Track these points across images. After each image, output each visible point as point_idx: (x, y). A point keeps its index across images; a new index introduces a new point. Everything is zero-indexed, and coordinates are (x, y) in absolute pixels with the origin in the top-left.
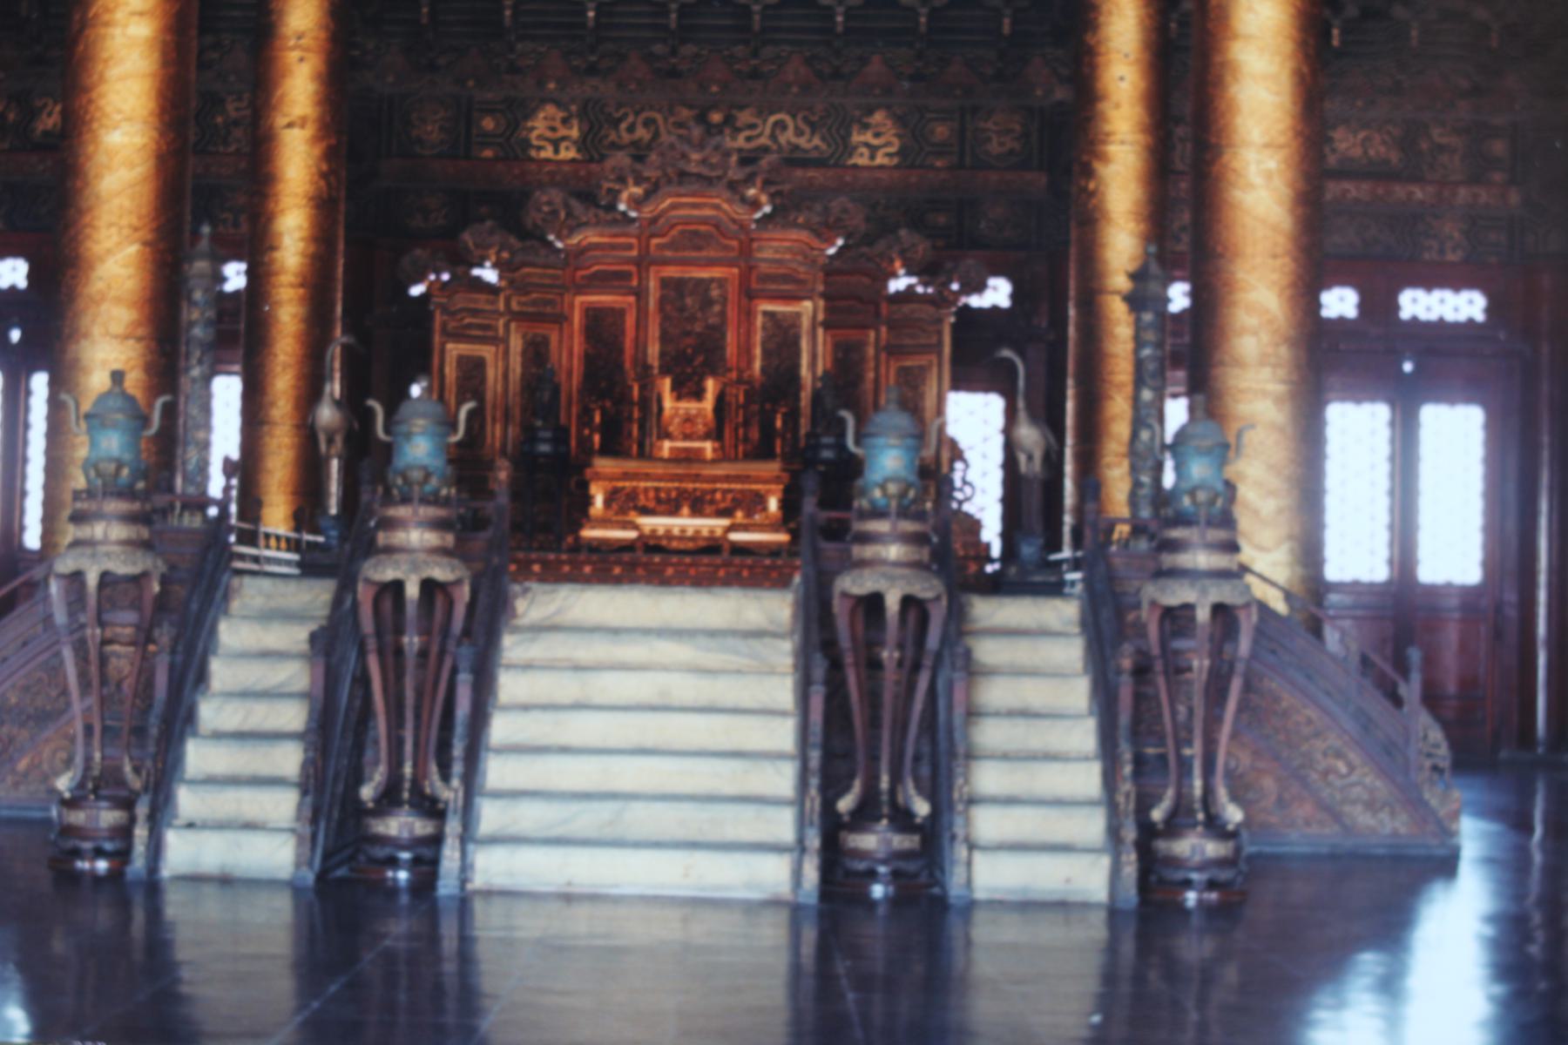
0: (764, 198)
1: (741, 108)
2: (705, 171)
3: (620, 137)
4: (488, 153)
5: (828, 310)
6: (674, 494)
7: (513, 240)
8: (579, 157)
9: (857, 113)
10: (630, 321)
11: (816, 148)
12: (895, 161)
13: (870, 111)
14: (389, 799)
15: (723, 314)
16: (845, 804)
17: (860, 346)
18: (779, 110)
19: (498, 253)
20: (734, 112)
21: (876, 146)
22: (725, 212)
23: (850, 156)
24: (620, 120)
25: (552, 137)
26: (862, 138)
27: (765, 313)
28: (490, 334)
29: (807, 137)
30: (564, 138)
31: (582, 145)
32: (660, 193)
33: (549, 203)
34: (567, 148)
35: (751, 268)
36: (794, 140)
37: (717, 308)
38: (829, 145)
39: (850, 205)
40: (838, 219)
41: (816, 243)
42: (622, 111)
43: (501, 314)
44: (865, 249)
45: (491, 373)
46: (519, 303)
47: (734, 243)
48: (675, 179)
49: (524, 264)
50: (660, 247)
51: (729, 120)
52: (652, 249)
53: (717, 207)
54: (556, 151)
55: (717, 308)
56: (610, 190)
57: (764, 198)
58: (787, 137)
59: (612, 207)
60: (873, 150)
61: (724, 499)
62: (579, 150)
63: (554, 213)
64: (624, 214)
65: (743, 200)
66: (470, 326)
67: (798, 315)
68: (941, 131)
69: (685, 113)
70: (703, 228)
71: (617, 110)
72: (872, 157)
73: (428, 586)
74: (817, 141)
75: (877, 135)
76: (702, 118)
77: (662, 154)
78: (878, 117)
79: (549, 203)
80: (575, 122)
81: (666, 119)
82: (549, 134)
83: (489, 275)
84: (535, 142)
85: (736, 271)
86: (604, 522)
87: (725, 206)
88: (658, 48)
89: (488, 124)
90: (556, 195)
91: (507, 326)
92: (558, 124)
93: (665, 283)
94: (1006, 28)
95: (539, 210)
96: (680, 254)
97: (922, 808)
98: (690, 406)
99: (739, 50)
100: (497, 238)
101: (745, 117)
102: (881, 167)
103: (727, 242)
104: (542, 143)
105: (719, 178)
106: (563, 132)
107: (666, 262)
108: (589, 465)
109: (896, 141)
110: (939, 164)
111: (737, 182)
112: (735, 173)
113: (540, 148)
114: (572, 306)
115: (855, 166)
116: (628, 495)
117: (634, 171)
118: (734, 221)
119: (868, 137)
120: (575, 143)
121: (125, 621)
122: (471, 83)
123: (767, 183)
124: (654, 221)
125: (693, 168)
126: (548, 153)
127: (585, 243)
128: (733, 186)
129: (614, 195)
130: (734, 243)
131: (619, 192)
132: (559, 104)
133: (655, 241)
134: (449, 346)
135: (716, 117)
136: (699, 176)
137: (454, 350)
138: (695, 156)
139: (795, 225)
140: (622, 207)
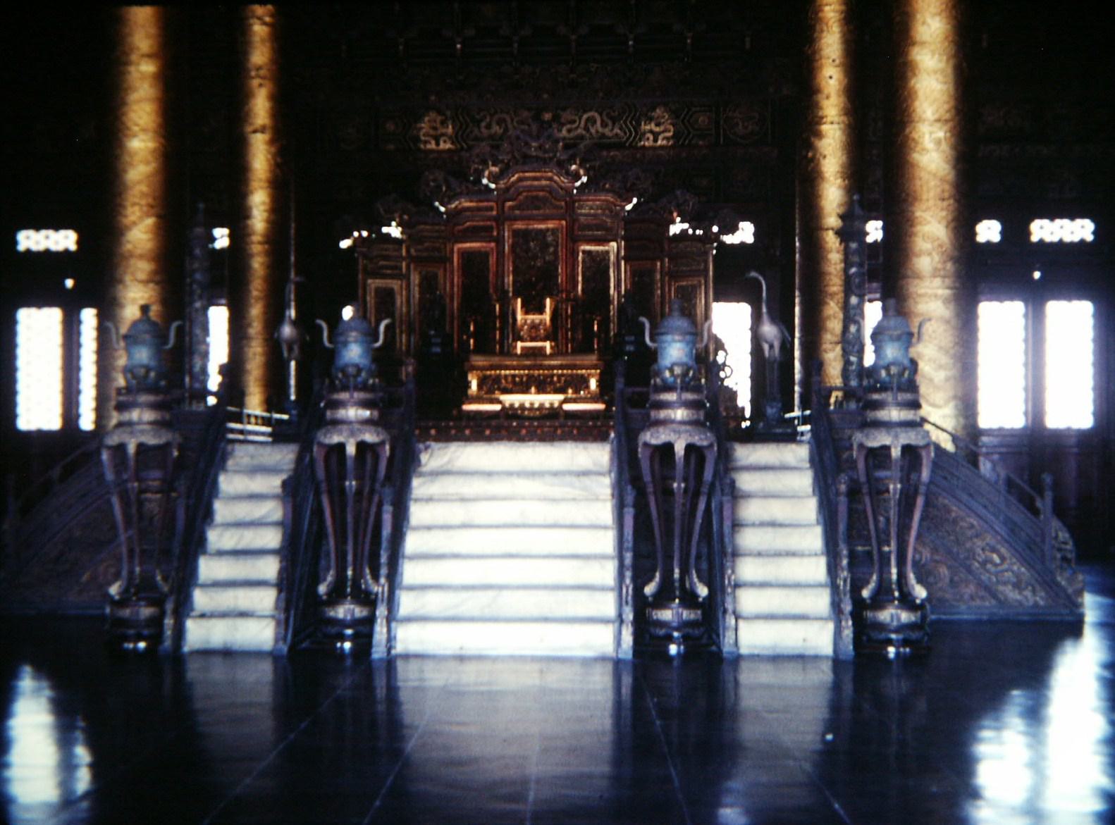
1: (564, 109)
2: (540, 154)
3: (481, 132)
4: (391, 147)
6: (525, 379)
9: (645, 109)
10: (492, 260)
13: (654, 109)
14: (337, 595)
15: (556, 252)
16: (649, 589)
17: (653, 271)
18: (591, 110)
19: (401, 217)
20: (559, 111)
22: (555, 182)
24: (481, 121)
26: (648, 127)
27: (584, 252)
28: (396, 272)
29: (610, 127)
30: (443, 135)
36: (600, 130)
37: (552, 249)
38: (625, 133)
42: (482, 114)
43: (404, 259)
44: (652, 205)
45: (399, 301)
46: (416, 251)
47: (563, 203)
49: (419, 223)
50: (512, 208)
51: (556, 118)
52: (506, 209)
54: (438, 144)
55: (552, 249)
56: (476, 170)
57: (582, 172)
61: (559, 380)
62: (453, 143)
63: (439, 187)
64: (487, 186)
65: (568, 173)
67: (607, 252)
68: (702, 119)
69: (526, 114)
70: (541, 194)
71: (478, 113)
72: (655, 140)
73: (361, 446)
74: (617, 130)
75: (658, 125)
76: (537, 117)
77: (511, 144)
78: (658, 111)
79: (434, 180)
81: (512, 120)
82: (432, 132)
83: (394, 231)
84: (423, 138)
85: (564, 223)
86: (478, 399)
87: (556, 178)
89: (390, 126)
93: (516, 233)
95: (428, 185)
97: (703, 591)
98: (536, 318)
101: (566, 115)
102: (662, 147)
103: (558, 203)
104: (427, 138)
105: (551, 159)
107: (516, 219)
108: (468, 360)
110: (701, 143)
111: (564, 161)
113: (426, 142)
115: (644, 146)
116: (494, 380)
117: (493, 155)
118: (562, 188)
119: (652, 126)
120: (450, 138)
121: (154, 477)
124: (507, 189)
126: (432, 146)
127: (460, 207)
129: (479, 175)
131: (483, 171)
132: (439, 112)
135: (547, 116)
136: (537, 158)
137: (373, 283)
139: (604, 190)
140: (485, 181)
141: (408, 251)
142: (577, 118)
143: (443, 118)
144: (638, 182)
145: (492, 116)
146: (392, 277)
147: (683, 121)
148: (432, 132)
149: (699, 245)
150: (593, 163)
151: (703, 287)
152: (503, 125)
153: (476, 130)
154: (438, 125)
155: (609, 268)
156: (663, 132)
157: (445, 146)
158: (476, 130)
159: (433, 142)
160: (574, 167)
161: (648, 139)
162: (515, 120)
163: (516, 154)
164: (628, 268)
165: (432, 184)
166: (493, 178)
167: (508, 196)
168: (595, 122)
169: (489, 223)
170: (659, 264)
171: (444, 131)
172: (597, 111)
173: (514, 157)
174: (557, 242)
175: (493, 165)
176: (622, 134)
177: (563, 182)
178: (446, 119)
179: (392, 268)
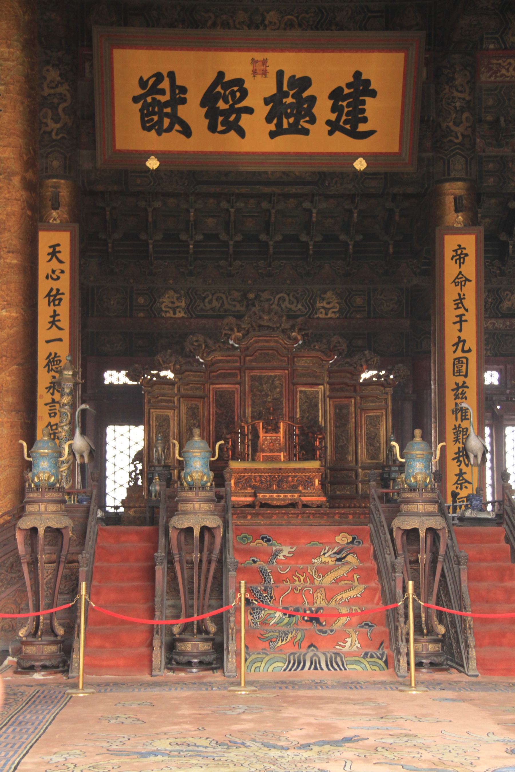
0: (299, 337)
1: (263, 291)
2: (270, 324)
3: (205, 306)
4: (141, 315)
5: (331, 390)
6: (268, 479)
7: (180, 359)
8: (186, 316)
9: (319, 292)
10: (237, 397)
11: (300, 309)
12: (337, 315)
13: (325, 292)
15: (281, 393)
17: (347, 406)
18: (281, 292)
19: (174, 365)
20: (260, 293)
21: (328, 308)
22: (280, 344)
23: (316, 313)
24: (205, 298)
25: (172, 306)
26: (321, 305)
27: (301, 392)
28: (171, 404)
29: (295, 304)
30: (178, 307)
31: (187, 310)
32: (249, 335)
33: (197, 341)
34: (180, 312)
35: (294, 370)
36: (289, 306)
37: (278, 390)
38: (306, 309)
39: (340, 340)
40: (335, 346)
41: (325, 358)
42: (206, 293)
43: (176, 395)
44: (348, 360)
46: (184, 389)
47: (286, 359)
48: (257, 328)
49: (186, 371)
50: (251, 361)
52: (247, 361)
53: (277, 342)
54: (175, 313)
55: (278, 390)
56: (225, 334)
57: (299, 337)
58: (286, 305)
59: (226, 342)
60: (327, 310)
61: (293, 481)
62: (185, 313)
63: (200, 346)
64: (232, 345)
65: (289, 338)
66: (161, 401)
67: (317, 392)
68: (359, 301)
69: (236, 294)
70: (270, 352)
71: (203, 293)
72: (326, 314)
74: (300, 306)
75: (328, 303)
76: (244, 296)
77: (250, 317)
78: (329, 294)
79: (197, 341)
80: (183, 299)
81: (227, 297)
82: (170, 305)
84: (164, 309)
85: (287, 372)
86: (237, 494)
87: (281, 341)
88: (222, 263)
89: (141, 300)
90: (201, 338)
91: (179, 400)
92: (175, 301)
93: (253, 379)
94: (391, 250)
95: (193, 344)
96: (259, 365)
98: (274, 436)
99: (261, 263)
100: (173, 358)
101: (265, 296)
102: (331, 318)
103: (283, 358)
104: (168, 309)
105: (278, 328)
106: (177, 304)
107: (253, 369)
109: (338, 306)
110: (358, 316)
111: (286, 329)
112: (286, 325)
113: (166, 312)
114: (209, 390)
115: (318, 318)
116: (246, 480)
117: (237, 325)
118: (285, 348)
119: (324, 304)
120: (183, 309)
122: (131, 281)
123: (300, 330)
124: (247, 349)
125: (265, 323)
126: (171, 314)
127: (214, 360)
128: (284, 331)
129: (228, 337)
130: (286, 359)
131: (230, 335)
132: (176, 292)
133: (248, 358)
134: (152, 410)
135: (251, 296)
136: (268, 327)
137: (154, 413)
138: (266, 317)
139: (314, 349)
140: (231, 342)
141: (179, 390)
142: (272, 298)
143: (179, 295)
144: (338, 345)
145: (213, 295)
146: (168, 408)
147: (345, 301)
148: (170, 305)
149: (382, 388)
150: (306, 332)
151: (384, 417)
152: (221, 301)
153: (202, 305)
154: (175, 301)
155: (318, 403)
156: (332, 308)
157: (180, 314)
158: (202, 305)
159: (171, 312)
160: (293, 334)
161: (321, 313)
162: (229, 298)
163: (254, 324)
164: (331, 403)
165: (195, 344)
166: (238, 340)
167: (248, 353)
168: (285, 300)
169: (234, 371)
170: (353, 401)
171: (179, 304)
172: (286, 293)
173: (252, 326)
174: (282, 385)
175: (238, 332)
176: (304, 309)
177: (286, 344)
178: (181, 296)
179: (168, 401)
